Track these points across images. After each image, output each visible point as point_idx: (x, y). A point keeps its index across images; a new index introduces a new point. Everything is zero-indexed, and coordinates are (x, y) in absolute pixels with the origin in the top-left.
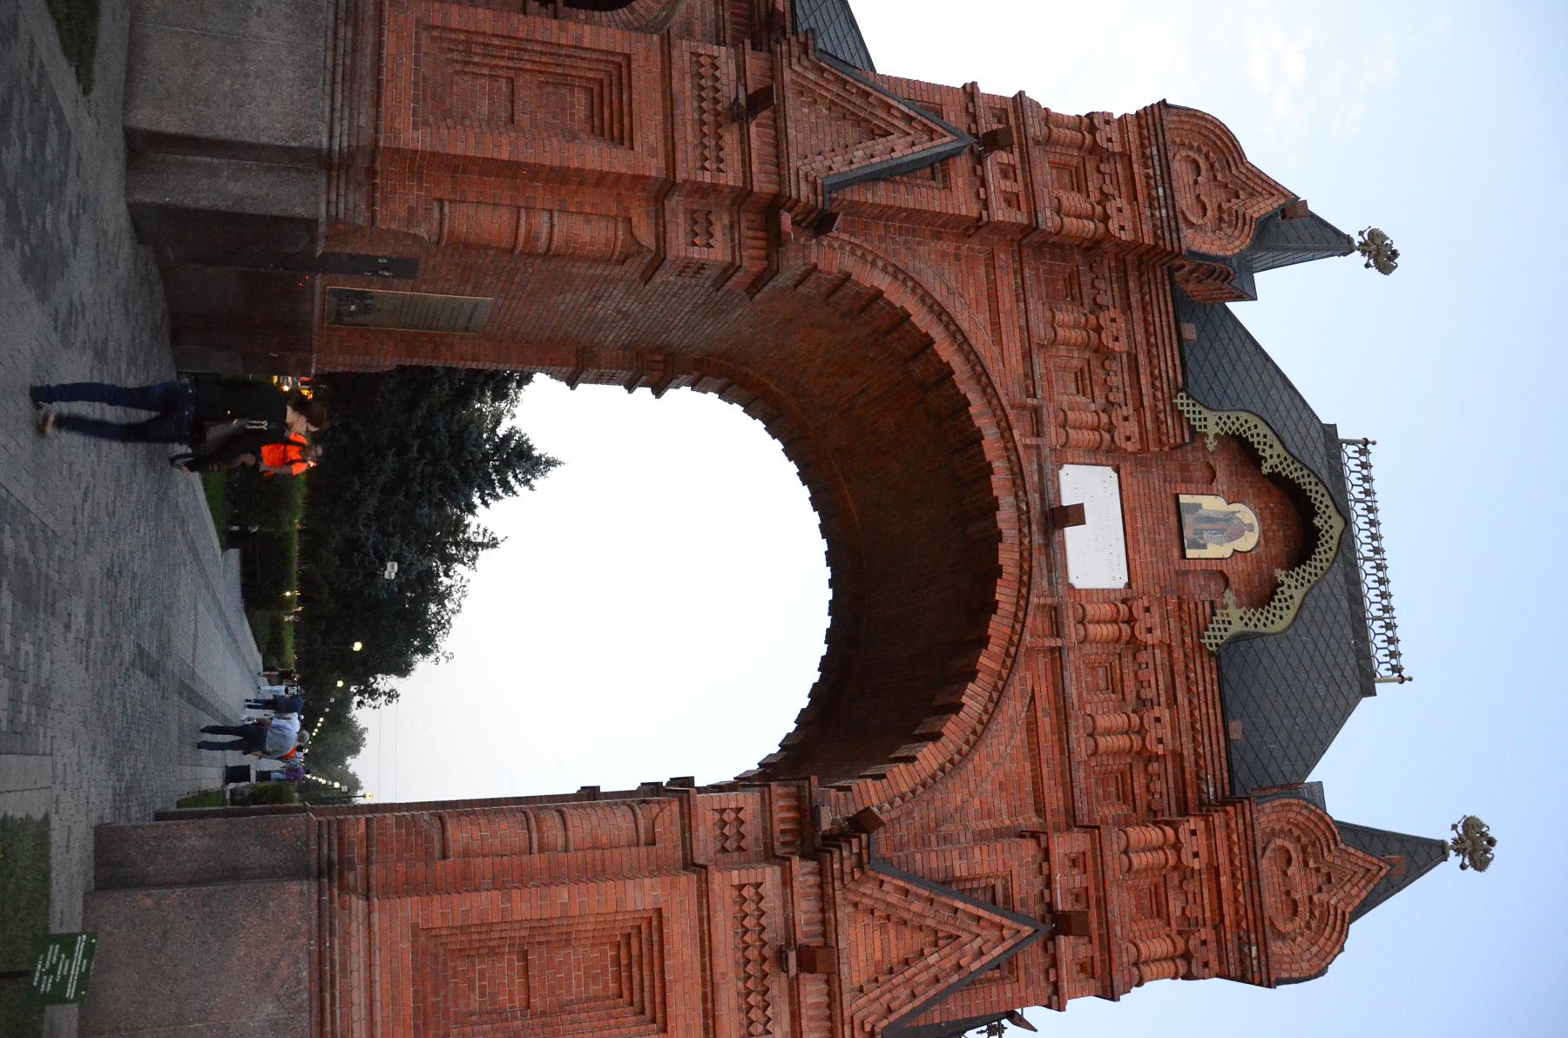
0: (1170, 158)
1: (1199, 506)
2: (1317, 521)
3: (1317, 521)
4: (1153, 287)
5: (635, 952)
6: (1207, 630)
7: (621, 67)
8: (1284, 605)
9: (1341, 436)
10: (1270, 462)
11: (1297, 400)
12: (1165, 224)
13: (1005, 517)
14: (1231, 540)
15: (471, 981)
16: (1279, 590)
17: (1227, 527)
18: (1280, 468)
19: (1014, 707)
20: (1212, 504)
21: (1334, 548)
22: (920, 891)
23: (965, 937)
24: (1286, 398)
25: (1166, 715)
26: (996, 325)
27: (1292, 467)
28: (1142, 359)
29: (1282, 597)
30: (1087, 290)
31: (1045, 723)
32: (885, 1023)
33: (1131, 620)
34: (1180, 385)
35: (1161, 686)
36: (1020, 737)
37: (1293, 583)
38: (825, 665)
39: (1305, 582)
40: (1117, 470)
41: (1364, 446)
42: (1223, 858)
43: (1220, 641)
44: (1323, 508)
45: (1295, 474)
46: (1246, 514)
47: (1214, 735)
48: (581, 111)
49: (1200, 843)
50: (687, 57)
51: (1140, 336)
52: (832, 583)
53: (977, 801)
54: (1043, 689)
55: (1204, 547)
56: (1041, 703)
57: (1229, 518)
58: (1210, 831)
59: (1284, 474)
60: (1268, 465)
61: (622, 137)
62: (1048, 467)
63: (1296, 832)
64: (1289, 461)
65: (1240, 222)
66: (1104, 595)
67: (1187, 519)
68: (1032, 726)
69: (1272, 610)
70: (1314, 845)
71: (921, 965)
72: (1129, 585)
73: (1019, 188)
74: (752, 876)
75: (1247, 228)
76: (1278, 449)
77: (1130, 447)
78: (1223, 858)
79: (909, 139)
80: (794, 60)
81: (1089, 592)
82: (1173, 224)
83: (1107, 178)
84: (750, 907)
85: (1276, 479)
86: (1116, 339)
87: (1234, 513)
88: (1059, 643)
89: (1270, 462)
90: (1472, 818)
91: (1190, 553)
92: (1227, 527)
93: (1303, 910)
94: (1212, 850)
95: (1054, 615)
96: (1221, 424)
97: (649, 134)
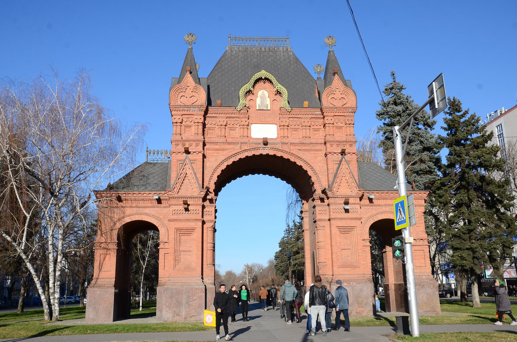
0: (182, 104)
1: (259, 104)
4: (212, 111)
5: (343, 231)
6: (287, 110)
7: (177, 229)
8: (281, 90)
10: (250, 88)
11: (223, 59)
12: (199, 108)
13: (264, 153)
14: (266, 98)
15: (346, 258)
16: (278, 90)
17: (263, 98)
18: (252, 85)
19: (301, 154)
20: (258, 101)
21: (270, 74)
22: (336, 180)
23: (344, 171)
25: (303, 120)
26: (223, 150)
27: (251, 82)
28: (228, 116)
29: (280, 90)
30: (211, 126)
31: (304, 148)
32: (358, 188)
34: (235, 108)
35: (297, 120)
36: (306, 153)
38: (277, 177)
39: (277, 85)
42: (333, 114)
43: (289, 107)
44: (260, 75)
46: (260, 93)
47: (307, 111)
48: (186, 237)
49: (330, 118)
50: (173, 216)
51: (223, 115)
52: (259, 174)
53: (318, 164)
54: (298, 148)
55: (267, 105)
56: (300, 148)
57: (261, 98)
58: (328, 116)
59: (253, 84)
60: (251, 88)
61: (193, 229)
62: (251, 141)
63: (328, 96)
64: (250, 82)
65: (196, 88)
68: (305, 150)
69: (283, 93)
70: (331, 92)
71: (348, 180)
73: (194, 143)
75: (197, 86)
78: (333, 114)
79: (188, 169)
80: (172, 194)
81: (278, 134)
82: (199, 107)
83: (187, 120)
87: (260, 96)
89: (250, 88)
91: (269, 109)
92: (263, 98)
93: (343, 96)
96: (243, 99)
97: (192, 225)
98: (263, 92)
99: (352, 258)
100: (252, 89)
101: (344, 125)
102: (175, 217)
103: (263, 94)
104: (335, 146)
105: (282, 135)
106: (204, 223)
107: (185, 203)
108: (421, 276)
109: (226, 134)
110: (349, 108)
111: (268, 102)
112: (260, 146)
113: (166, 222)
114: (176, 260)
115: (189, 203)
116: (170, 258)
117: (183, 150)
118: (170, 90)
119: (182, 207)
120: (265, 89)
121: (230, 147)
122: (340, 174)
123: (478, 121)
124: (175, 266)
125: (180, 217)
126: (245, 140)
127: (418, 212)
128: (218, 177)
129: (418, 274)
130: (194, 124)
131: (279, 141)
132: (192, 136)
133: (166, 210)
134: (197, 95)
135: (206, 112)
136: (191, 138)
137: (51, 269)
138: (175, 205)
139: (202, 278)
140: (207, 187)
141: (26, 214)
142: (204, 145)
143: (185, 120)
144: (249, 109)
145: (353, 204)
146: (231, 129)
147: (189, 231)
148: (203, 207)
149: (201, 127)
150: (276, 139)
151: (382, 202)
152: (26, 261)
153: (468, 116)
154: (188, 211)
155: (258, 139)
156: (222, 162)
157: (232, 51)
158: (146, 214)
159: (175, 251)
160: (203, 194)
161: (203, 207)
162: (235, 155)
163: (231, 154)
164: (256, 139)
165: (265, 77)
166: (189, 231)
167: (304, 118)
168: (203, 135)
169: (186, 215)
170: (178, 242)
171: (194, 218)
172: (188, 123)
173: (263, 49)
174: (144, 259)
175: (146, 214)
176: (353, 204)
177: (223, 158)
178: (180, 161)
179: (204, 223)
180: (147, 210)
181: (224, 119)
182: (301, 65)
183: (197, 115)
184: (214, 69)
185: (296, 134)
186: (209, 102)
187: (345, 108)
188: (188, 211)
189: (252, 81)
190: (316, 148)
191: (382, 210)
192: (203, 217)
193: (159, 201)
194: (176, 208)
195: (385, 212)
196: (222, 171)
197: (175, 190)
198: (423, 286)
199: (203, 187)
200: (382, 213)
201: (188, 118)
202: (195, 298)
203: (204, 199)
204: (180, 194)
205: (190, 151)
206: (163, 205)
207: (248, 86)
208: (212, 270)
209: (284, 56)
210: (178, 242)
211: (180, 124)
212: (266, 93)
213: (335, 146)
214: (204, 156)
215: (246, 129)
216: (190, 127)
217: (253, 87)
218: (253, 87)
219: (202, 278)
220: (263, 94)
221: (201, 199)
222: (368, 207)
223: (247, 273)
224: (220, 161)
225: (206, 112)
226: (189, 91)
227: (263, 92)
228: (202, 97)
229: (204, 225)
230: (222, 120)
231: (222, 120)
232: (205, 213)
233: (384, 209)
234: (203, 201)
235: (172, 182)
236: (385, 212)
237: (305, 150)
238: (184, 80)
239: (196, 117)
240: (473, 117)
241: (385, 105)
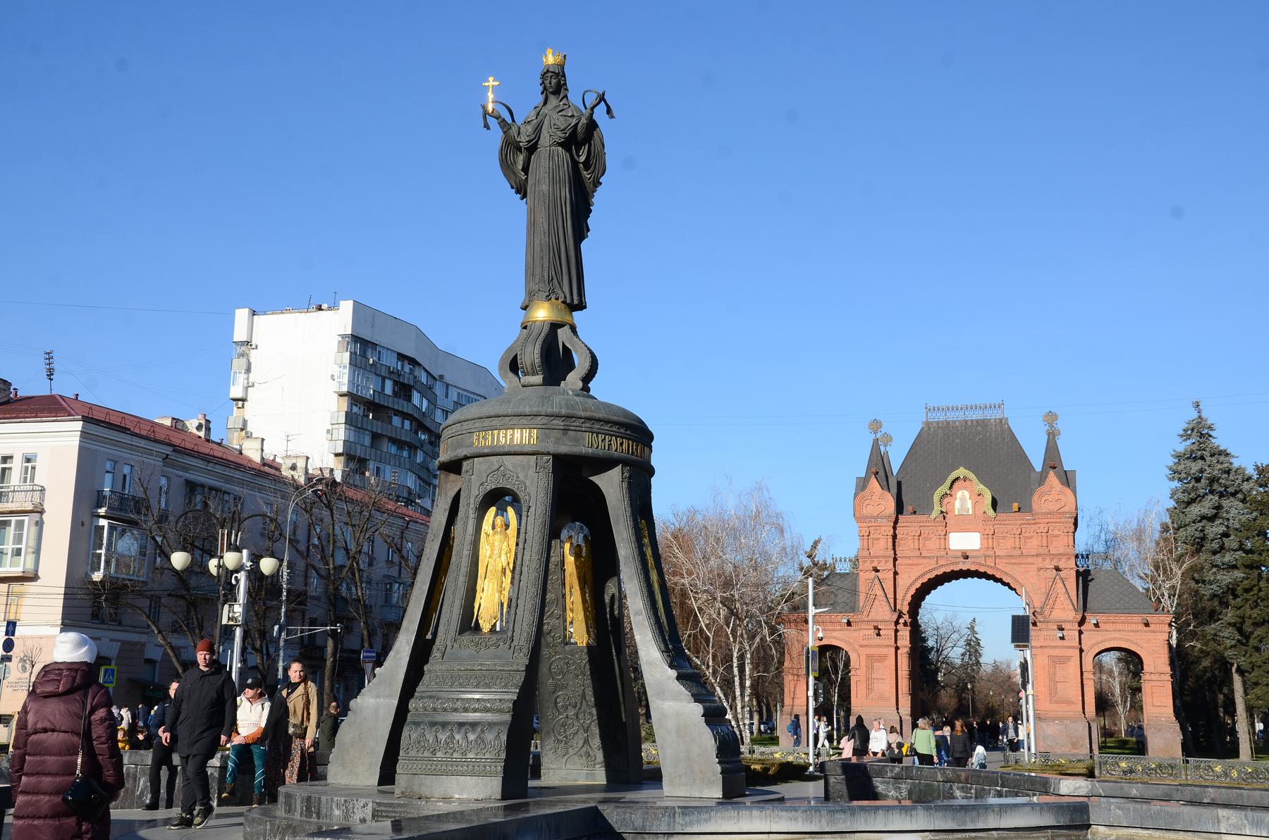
7: (868, 656)
17: (963, 500)
19: (1008, 569)
20: (957, 504)
26: (917, 565)
28: (921, 524)
36: (1015, 566)
46: (959, 494)
48: (878, 664)
57: (961, 500)
61: (886, 656)
66: (982, 539)
68: (1013, 564)
73: (883, 560)
78: (1047, 521)
81: (981, 544)
91: (970, 513)
92: (963, 500)
93: (1060, 497)
97: (884, 651)
98: (963, 493)
99: (1158, 684)
100: (948, 492)
101: (1061, 533)
102: (865, 642)
103: (963, 496)
104: (1048, 561)
106: (897, 648)
107: (876, 628)
108: (1160, 717)
109: (920, 546)
110: (1066, 513)
111: (969, 505)
112: (958, 560)
113: (857, 647)
114: (869, 689)
115: (879, 627)
116: (862, 686)
117: (872, 569)
118: (854, 499)
119: (872, 632)
120: (965, 488)
121: (925, 561)
122: (1053, 595)
124: (867, 695)
125: (871, 642)
127: (1158, 639)
128: (912, 596)
129: (1156, 715)
130: (883, 537)
131: (981, 553)
132: (881, 550)
133: (856, 634)
135: (896, 522)
136: (881, 553)
137: (738, 693)
138: (865, 629)
139: (897, 709)
140: (899, 610)
141: (708, 634)
142: (895, 560)
143: (872, 532)
144: (947, 513)
145: (1069, 630)
146: (925, 539)
147: (883, 658)
148: (896, 631)
149: (890, 540)
150: (978, 550)
151: (1107, 627)
152: (715, 685)
154: (880, 636)
155: (957, 551)
156: (917, 579)
157: (929, 428)
158: (835, 638)
159: (868, 679)
160: (895, 617)
161: (896, 631)
162: (930, 571)
163: (927, 569)
164: (955, 550)
166: (883, 658)
167: (1014, 525)
168: (894, 549)
169: (878, 641)
170: (870, 668)
171: (886, 644)
172: (876, 536)
173: (969, 423)
174: (836, 673)
175: (835, 638)
176: (1069, 630)
177: (917, 574)
178: (869, 580)
179: (897, 648)
180: (836, 634)
181: (917, 529)
183: (886, 526)
185: (1004, 543)
186: (900, 509)
187: (1060, 513)
188: (880, 636)
189: (948, 482)
190: (1027, 562)
191: (1110, 636)
192: (896, 642)
193: (849, 624)
194: (867, 632)
195: (1115, 639)
196: (917, 589)
197: (865, 613)
198: (1160, 730)
199: (895, 610)
200: (1110, 640)
201: (876, 530)
203: (897, 623)
204: (870, 618)
205: (878, 568)
206: (852, 628)
207: (944, 489)
208: (907, 700)
209: (996, 431)
210: (870, 668)
211: (867, 538)
212: (967, 494)
213: (1048, 561)
214: (896, 573)
216: (878, 539)
217: (951, 488)
218: (951, 488)
219: (897, 709)
220: (963, 496)
221: (893, 623)
222: (1092, 633)
223: (1116, 674)
224: (914, 578)
225: (896, 522)
226: (876, 497)
227: (963, 493)
228: (890, 504)
229: (899, 651)
230: (914, 530)
231: (914, 530)
232: (899, 637)
233: (1114, 635)
234: (896, 626)
235: (861, 605)
236: (1115, 639)
237: (1013, 564)
238: (870, 486)
239: (884, 528)
241: (1179, 457)
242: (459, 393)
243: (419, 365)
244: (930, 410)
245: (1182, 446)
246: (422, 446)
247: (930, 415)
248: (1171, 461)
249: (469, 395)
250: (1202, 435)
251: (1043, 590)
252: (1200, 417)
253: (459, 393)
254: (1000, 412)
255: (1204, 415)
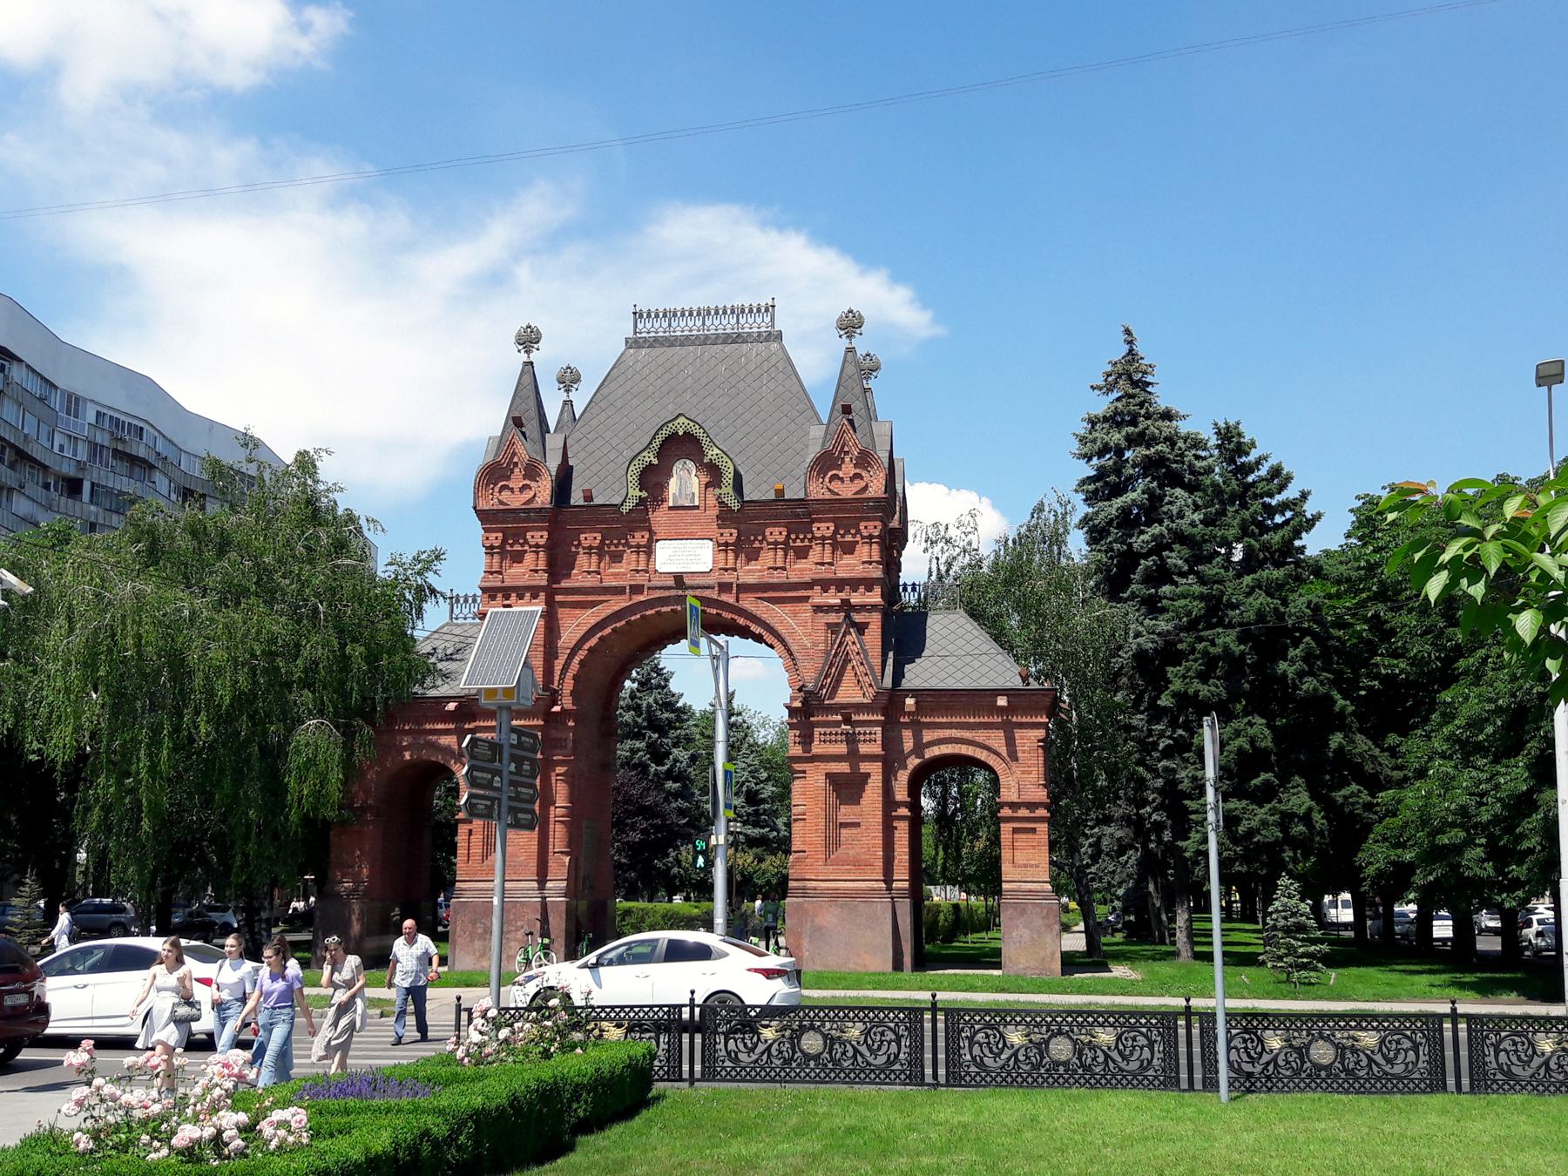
2: (681, 433)
3: (681, 433)
9: (631, 335)
10: (652, 458)
24: (614, 385)
33: (727, 544)
37: (710, 452)
40: (657, 541)
41: (637, 315)
45: (657, 444)
49: (823, 525)
55: (693, 494)
58: (820, 520)
67: (680, 503)
72: (711, 540)
74: (816, 735)
76: (645, 454)
77: (647, 536)
84: (833, 737)
85: (659, 455)
86: (595, 538)
88: (734, 585)
89: (652, 458)
90: (840, 320)
91: (697, 503)
94: (826, 520)
95: (724, 587)
105: (722, 565)
123: (1289, 478)
126: (640, 579)
134: (533, 484)
153: (1263, 471)
165: (685, 432)
182: (795, 380)
184: (591, 401)
202: (519, 923)
215: (643, 557)
240: (1276, 472)
241: (1093, 422)
242: (98, 412)
243: (20, 361)
244: (641, 316)
245: (1102, 405)
246: (22, 487)
247: (640, 326)
248: (1082, 428)
249: (116, 415)
250: (1135, 384)
251: (822, 647)
252: (1131, 351)
253: (98, 412)
254: (767, 320)
255: (1140, 348)
